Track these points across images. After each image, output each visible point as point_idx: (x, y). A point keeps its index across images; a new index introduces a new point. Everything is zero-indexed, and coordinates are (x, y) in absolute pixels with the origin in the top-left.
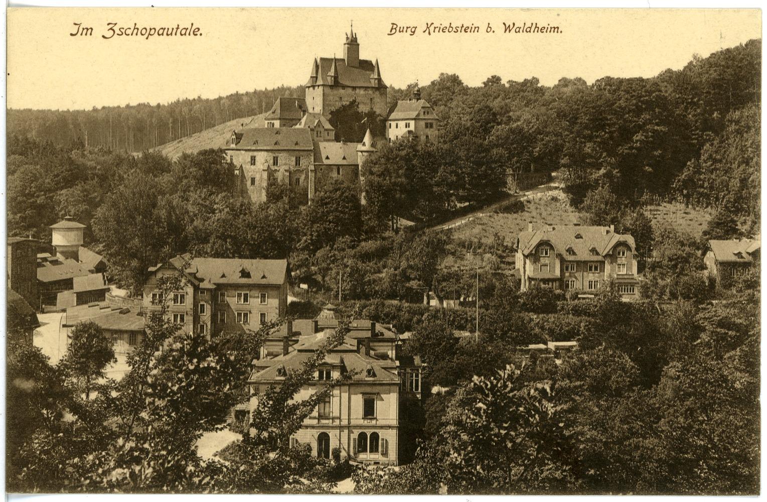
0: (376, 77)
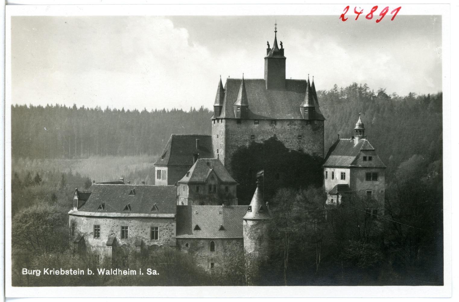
0: (306, 105)
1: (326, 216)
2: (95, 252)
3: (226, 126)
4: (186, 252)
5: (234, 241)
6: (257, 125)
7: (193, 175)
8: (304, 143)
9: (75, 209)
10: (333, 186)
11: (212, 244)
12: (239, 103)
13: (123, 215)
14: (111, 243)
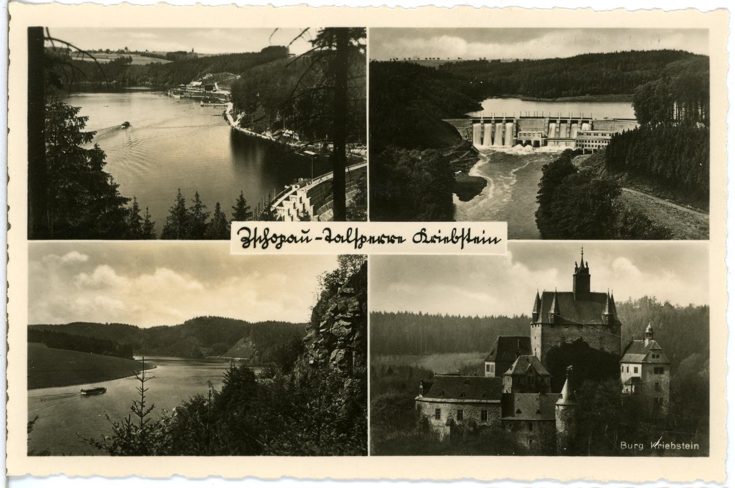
0: (606, 313)
1: (622, 403)
2: (437, 430)
3: (542, 330)
4: (510, 431)
5: (548, 423)
6: (567, 329)
7: (516, 368)
8: (604, 343)
9: (421, 396)
10: (628, 378)
11: (530, 424)
12: (552, 311)
13: (459, 401)
14: (450, 423)
